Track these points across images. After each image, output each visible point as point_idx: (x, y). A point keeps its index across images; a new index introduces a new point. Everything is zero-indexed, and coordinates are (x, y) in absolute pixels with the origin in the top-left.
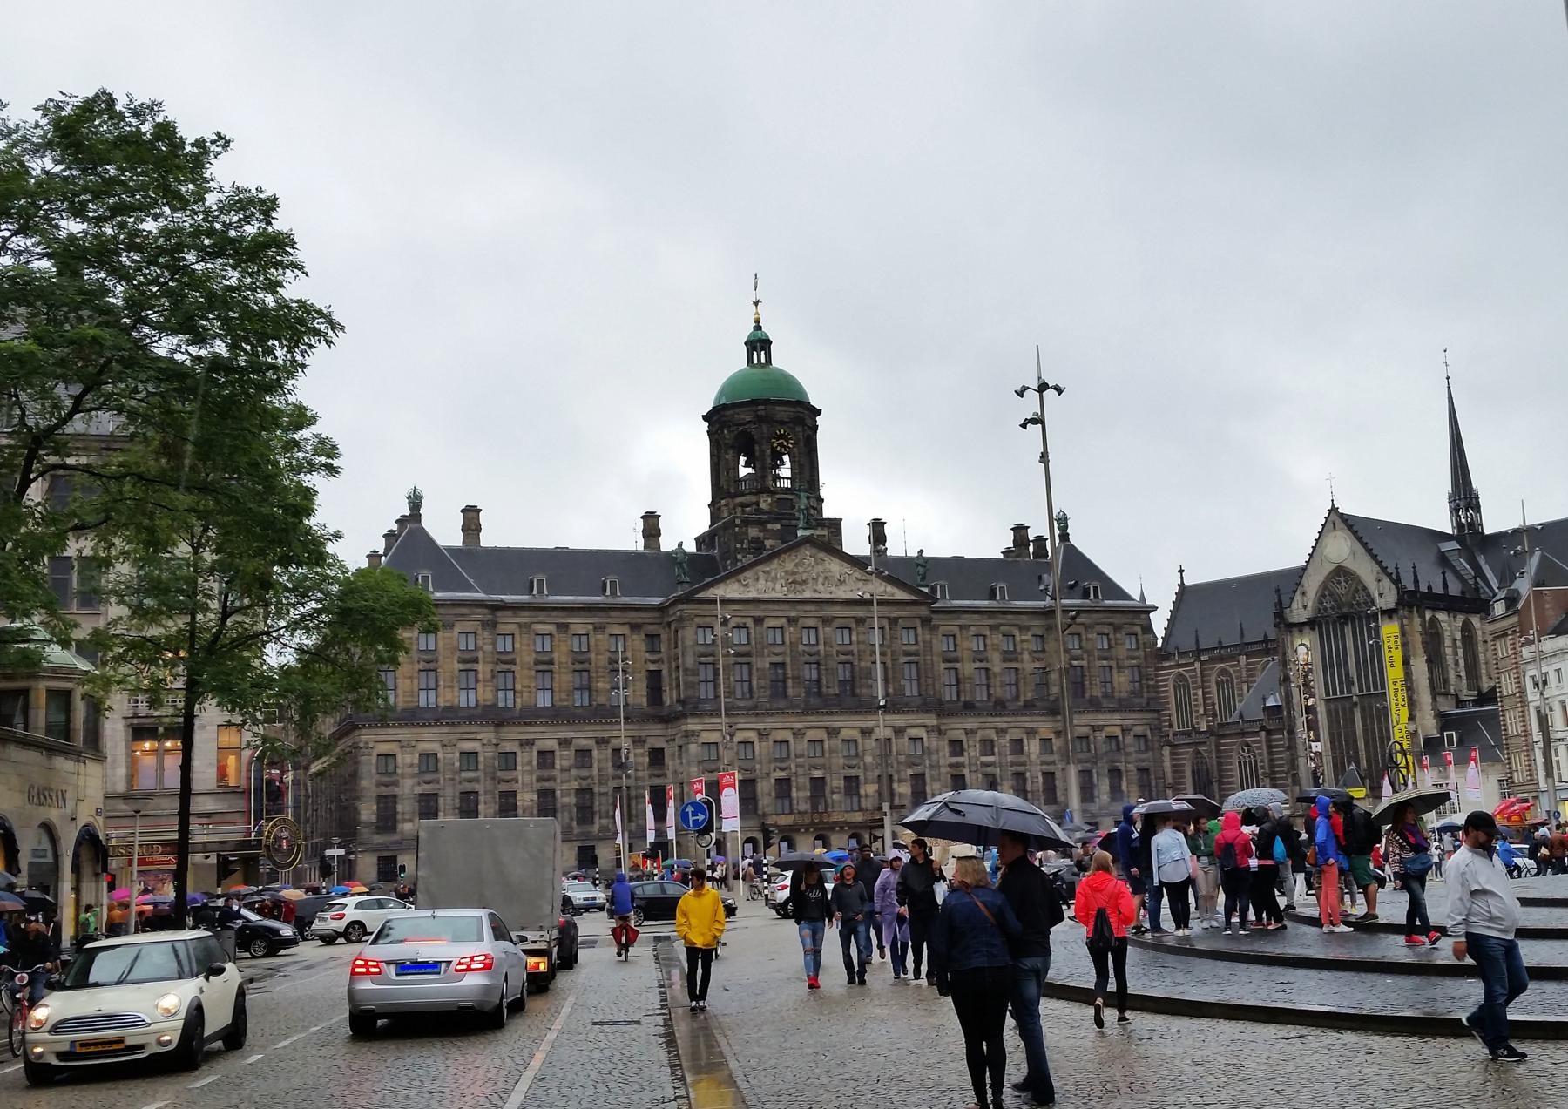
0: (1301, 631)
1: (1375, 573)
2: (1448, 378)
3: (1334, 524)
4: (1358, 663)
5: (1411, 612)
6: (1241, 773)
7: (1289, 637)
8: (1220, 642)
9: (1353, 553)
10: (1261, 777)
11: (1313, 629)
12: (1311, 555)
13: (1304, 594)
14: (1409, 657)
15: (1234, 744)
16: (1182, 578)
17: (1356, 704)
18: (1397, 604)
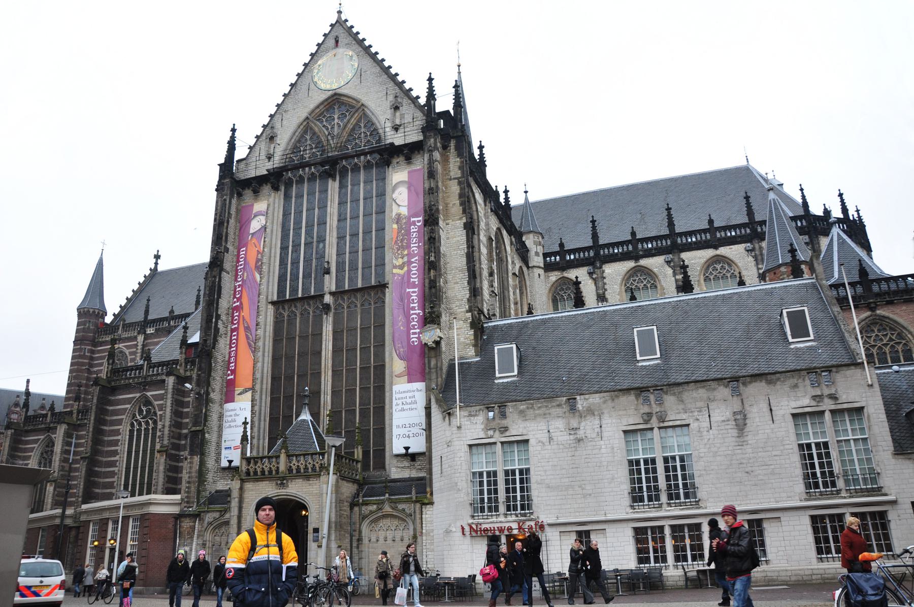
0: (256, 192)
1: (391, 98)
2: (459, 66)
3: (337, 42)
4: (341, 238)
5: (445, 147)
6: (130, 453)
7: (234, 201)
8: (172, 312)
9: (360, 73)
10: (157, 455)
11: (276, 188)
12: (292, 86)
13: (272, 139)
14: (438, 210)
15: (128, 401)
16: (156, 264)
17: (327, 308)
18: (424, 130)
